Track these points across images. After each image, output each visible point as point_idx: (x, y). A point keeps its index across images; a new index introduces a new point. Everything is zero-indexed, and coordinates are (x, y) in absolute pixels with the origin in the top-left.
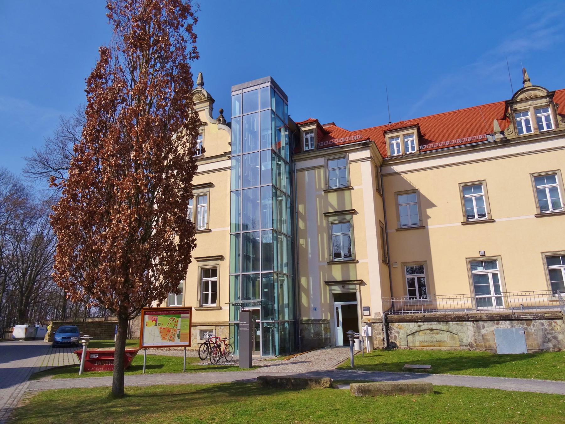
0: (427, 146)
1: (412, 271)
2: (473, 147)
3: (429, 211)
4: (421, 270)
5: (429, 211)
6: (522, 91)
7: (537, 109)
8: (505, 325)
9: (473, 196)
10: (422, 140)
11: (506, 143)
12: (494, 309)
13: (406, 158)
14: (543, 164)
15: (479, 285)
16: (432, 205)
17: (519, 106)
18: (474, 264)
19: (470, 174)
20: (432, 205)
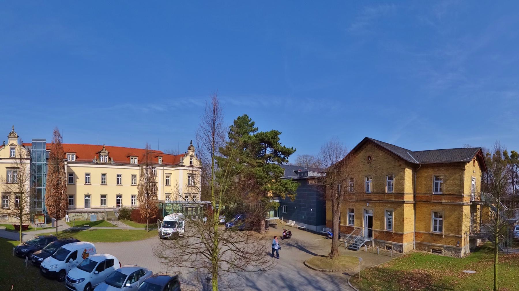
0: (79, 160)
1: (70, 197)
2: (90, 163)
3: (77, 180)
4: (72, 196)
5: (77, 180)
6: (103, 150)
7: (105, 156)
8: (93, 214)
9: (88, 177)
10: (77, 157)
11: (97, 164)
12: (89, 209)
13: (72, 162)
14: (104, 171)
15: (87, 202)
16: (78, 178)
17: (101, 154)
18: (86, 196)
19: (88, 171)
20: (78, 178)
